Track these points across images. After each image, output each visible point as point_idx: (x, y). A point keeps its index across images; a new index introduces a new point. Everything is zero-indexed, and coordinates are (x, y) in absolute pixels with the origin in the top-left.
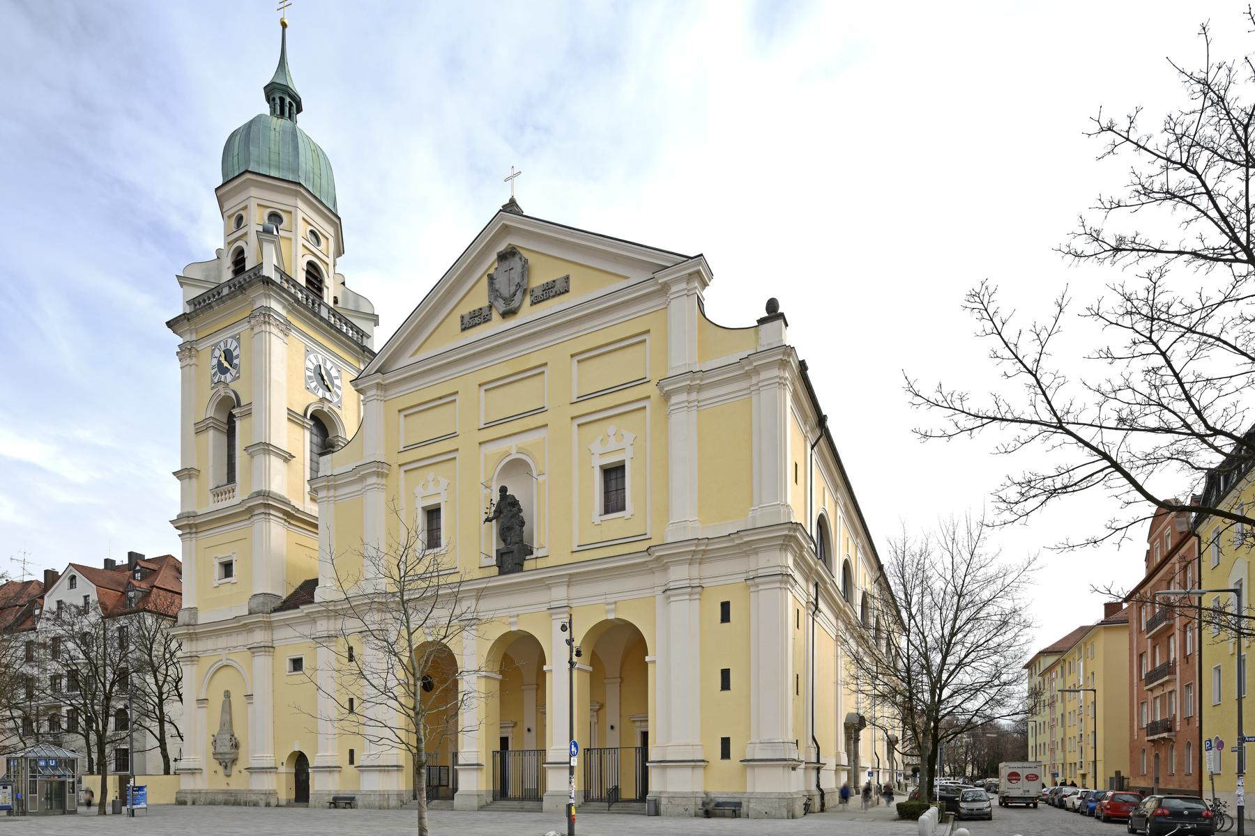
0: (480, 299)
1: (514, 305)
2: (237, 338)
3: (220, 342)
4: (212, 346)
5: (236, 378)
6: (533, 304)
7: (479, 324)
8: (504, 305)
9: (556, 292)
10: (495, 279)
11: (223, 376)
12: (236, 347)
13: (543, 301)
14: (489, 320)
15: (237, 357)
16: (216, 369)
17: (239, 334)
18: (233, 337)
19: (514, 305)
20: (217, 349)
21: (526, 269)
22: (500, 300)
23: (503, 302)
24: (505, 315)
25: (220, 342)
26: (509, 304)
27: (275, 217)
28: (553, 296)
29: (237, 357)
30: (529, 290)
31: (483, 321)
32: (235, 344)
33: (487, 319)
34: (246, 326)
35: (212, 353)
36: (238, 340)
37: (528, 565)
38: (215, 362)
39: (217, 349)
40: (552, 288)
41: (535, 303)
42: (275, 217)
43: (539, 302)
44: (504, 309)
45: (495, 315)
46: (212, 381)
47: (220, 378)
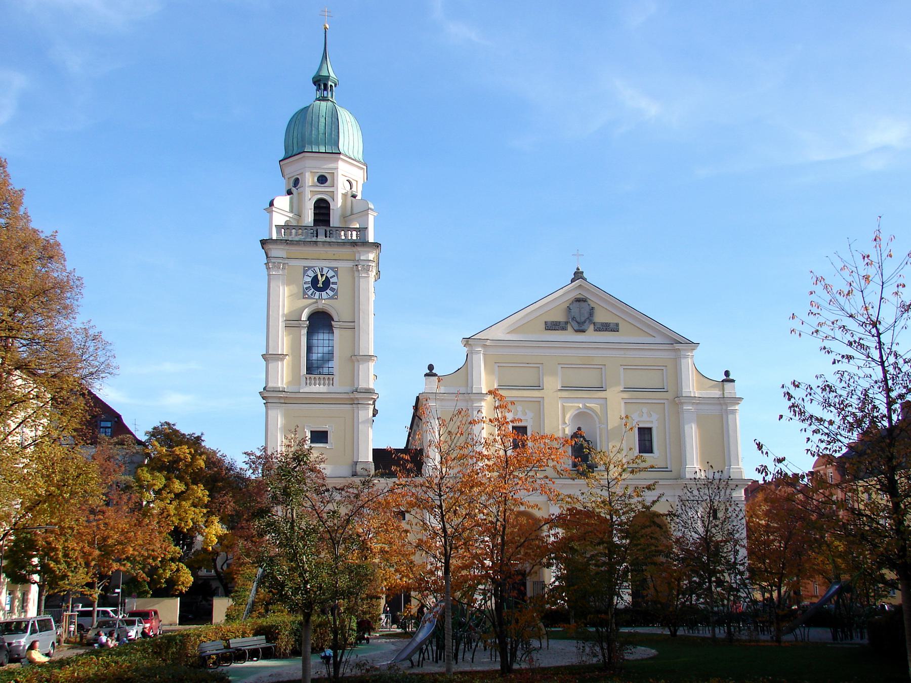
0: (560, 317)
1: (583, 327)
4: (304, 267)
5: (332, 298)
6: (595, 330)
12: (334, 276)
15: (333, 283)
17: (337, 268)
18: (332, 269)
19: (583, 327)
24: (577, 331)
34: (350, 264)
36: (336, 272)
38: (309, 279)
46: (305, 293)
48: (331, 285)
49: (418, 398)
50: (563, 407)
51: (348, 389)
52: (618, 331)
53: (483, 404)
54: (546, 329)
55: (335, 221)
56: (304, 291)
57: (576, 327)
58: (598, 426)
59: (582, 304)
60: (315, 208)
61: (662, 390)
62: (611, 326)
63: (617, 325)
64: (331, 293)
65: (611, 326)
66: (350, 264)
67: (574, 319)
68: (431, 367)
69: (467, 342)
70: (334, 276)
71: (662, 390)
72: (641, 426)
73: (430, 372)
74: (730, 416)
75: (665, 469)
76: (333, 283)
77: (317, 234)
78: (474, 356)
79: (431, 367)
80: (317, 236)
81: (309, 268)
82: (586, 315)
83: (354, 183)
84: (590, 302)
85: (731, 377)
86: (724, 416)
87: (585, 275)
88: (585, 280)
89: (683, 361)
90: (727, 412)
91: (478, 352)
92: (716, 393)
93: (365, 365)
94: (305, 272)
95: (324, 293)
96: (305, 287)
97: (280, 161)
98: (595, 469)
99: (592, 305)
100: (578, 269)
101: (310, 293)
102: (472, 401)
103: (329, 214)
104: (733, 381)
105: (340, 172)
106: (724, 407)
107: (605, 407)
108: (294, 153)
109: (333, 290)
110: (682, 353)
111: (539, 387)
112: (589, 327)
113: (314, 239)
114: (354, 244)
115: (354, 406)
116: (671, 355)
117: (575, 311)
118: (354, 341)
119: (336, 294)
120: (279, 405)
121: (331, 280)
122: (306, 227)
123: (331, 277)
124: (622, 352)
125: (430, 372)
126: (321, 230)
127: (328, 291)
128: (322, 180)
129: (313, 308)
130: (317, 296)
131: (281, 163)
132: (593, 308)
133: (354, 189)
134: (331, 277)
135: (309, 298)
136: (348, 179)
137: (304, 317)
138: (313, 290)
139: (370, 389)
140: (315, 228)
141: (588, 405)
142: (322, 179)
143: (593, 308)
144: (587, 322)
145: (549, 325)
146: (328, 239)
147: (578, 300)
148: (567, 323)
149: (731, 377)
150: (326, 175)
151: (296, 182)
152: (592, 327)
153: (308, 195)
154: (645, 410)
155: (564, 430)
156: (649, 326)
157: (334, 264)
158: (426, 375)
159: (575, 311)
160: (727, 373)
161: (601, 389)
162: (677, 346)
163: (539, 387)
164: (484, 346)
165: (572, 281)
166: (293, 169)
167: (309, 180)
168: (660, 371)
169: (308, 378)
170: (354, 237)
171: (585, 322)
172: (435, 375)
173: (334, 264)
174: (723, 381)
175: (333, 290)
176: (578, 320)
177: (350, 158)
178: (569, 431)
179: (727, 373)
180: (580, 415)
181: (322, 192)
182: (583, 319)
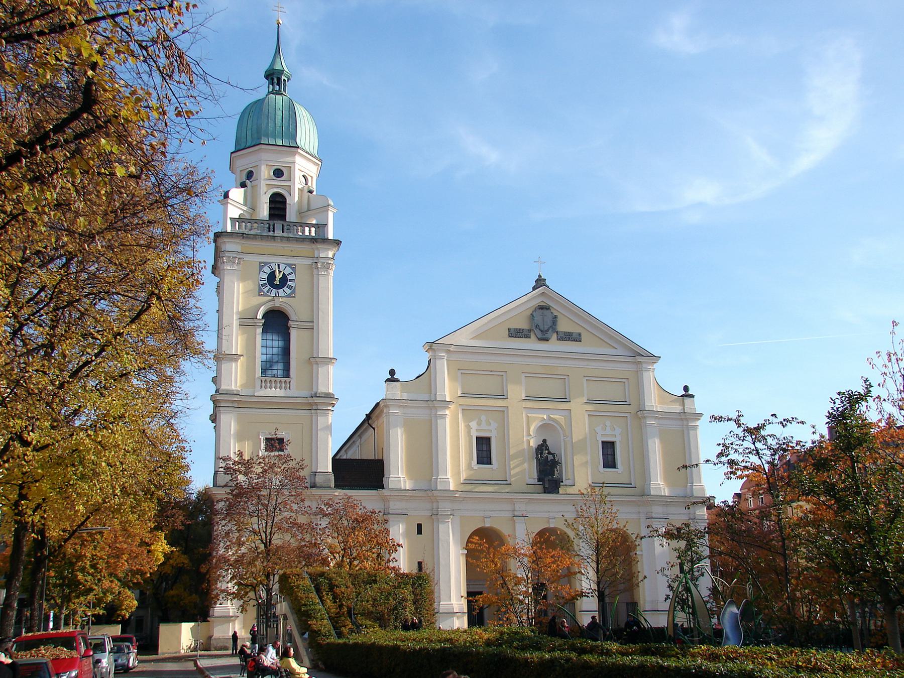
0: (523, 325)
1: (547, 336)
4: (260, 263)
5: (289, 296)
6: (558, 339)
12: (291, 273)
15: (291, 281)
16: (266, 282)
18: (290, 265)
19: (547, 336)
33: (528, 337)
34: (308, 262)
35: (261, 267)
36: (294, 269)
37: (561, 490)
38: (266, 276)
46: (260, 290)
48: (288, 283)
49: (378, 404)
51: (305, 393)
52: (580, 341)
53: (447, 412)
54: (509, 336)
55: (291, 216)
56: (259, 287)
57: (540, 335)
58: (562, 438)
59: (546, 312)
60: (271, 202)
61: (625, 403)
62: (574, 334)
63: (580, 335)
64: (288, 291)
66: (308, 262)
67: (537, 326)
68: (392, 372)
69: (431, 346)
70: (291, 273)
71: (625, 403)
72: (605, 440)
73: (392, 378)
74: (691, 432)
75: (628, 485)
76: (291, 281)
77: (274, 228)
78: (438, 362)
79: (392, 372)
80: (274, 231)
81: (266, 264)
82: (550, 324)
83: (309, 179)
84: (552, 310)
85: (690, 392)
86: (685, 432)
87: (547, 283)
88: (548, 287)
89: (645, 374)
90: (689, 428)
91: (441, 358)
92: (677, 408)
93: (325, 368)
94: (261, 267)
95: (280, 291)
97: (231, 153)
98: (561, 483)
99: (555, 313)
100: (540, 276)
101: (265, 290)
102: (436, 408)
103: (285, 209)
104: (692, 396)
105: (297, 167)
106: (685, 423)
107: (569, 419)
108: (248, 144)
109: (290, 287)
110: (644, 366)
111: (503, 396)
112: (552, 336)
113: (271, 233)
114: (313, 240)
115: (313, 411)
116: (632, 368)
117: (538, 319)
119: (294, 292)
120: (232, 409)
121: (289, 277)
122: (262, 222)
123: (289, 275)
124: (586, 363)
125: (392, 378)
126: (278, 224)
127: (285, 289)
128: (278, 174)
129: (269, 306)
130: (273, 294)
131: (233, 155)
132: (556, 317)
133: (310, 184)
134: (289, 275)
135: (265, 295)
136: (304, 174)
137: (260, 316)
138: (269, 287)
139: (330, 394)
140: (271, 223)
141: (552, 416)
142: (278, 173)
143: (556, 317)
145: (512, 332)
146: (285, 235)
147: (541, 308)
148: (530, 331)
149: (690, 392)
150: (282, 168)
151: (250, 175)
152: (555, 336)
153: (263, 188)
154: (608, 423)
155: (529, 442)
157: (291, 261)
158: (388, 380)
159: (538, 319)
160: (686, 388)
161: (565, 400)
162: (639, 359)
163: (503, 396)
164: (448, 351)
165: (534, 289)
166: (245, 161)
167: (265, 173)
168: (622, 384)
169: (263, 380)
170: (313, 234)
171: (548, 330)
172: (397, 380)
173: (291, 261)
174: (682, 396)
175: (290, 287)
176: (542, 329)
177: (307, 153)
178: (534, 443)
179: (686, 388)
180: (545, 427)
181: (278, 185)
182: (546, 327)
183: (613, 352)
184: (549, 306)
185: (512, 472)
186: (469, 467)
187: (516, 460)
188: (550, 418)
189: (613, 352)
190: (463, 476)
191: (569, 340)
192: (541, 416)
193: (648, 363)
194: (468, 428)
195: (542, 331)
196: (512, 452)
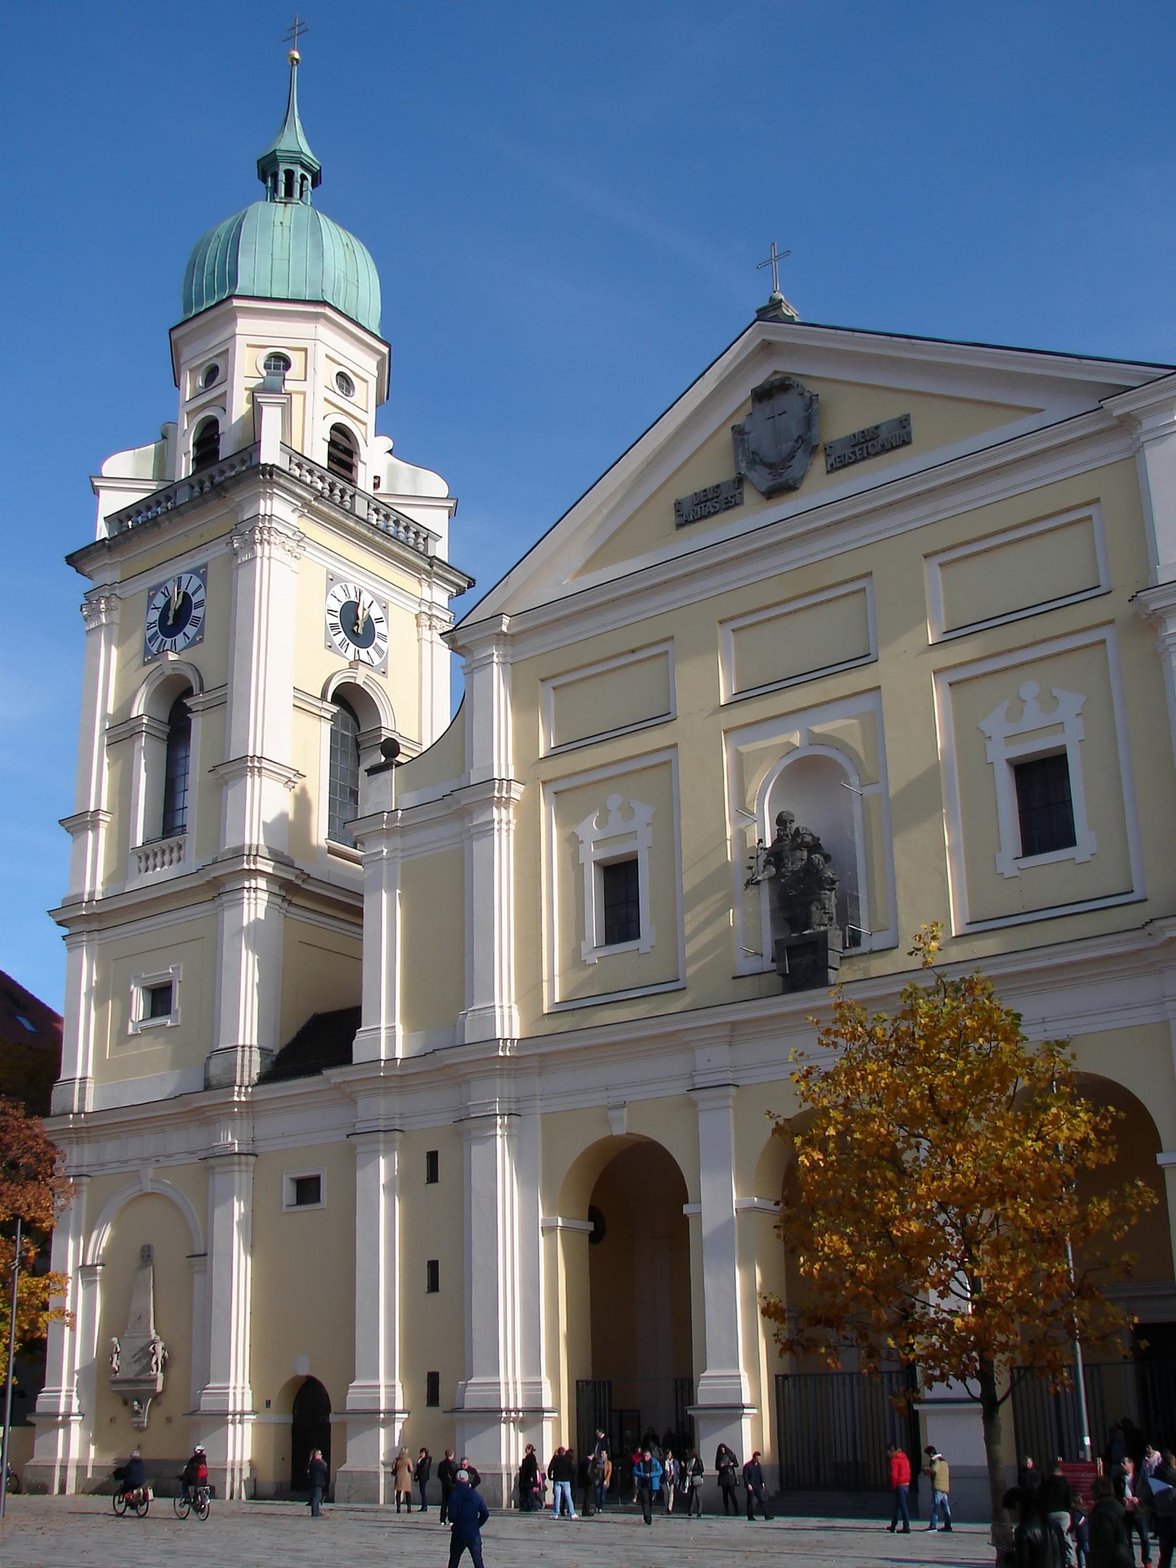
1: (789, 475)
2: (201, 573)
3: (169, 580)
4: (150, 590)
5: (193, 643)
6: (832, 469)
7: (715, 513)
8: (770, 477)
9: (883, 446)
10: (748, 433)
11: (169, 640)
13: (853, 463)
14: (736, 505)
15: (200, 604)
16: (157, 628)
17: (205, 566)
18: (195, 571)
20: (160, 594)
21: (811, 409)
22: (760, 468)
23: (768, 471)
24: (772, 494)
25: (169, 580)
26: (781, 475)
27: (279, 362)
28: (877, 454)
29: (200, 604)
30: (821, 447)
31: (724, 506)
32: (196, 581)
35: (151, 599)
36: (203, 577)
38: (155, 616)
39: (160, 594)
40: (872, 439)
41: (838, 468)
42: (279, 362)
43: (845, 466)
44: (771, 483)
45: (750, 496)
46: (147, 651)
47: (163, 643)
50: (739, 760)
61: (1093, 592)
62: (884, 434)
65: (884, 434)
67: (755, 460)
71: (1093, 592)
81: (156, 589)
94: (151, 599)
96: (148, 637)
99: (812, 387)
101: (154, 650)
107: (874, 725)
118: (223, 733)
121: (195, 600)
138: (162, 637)
141: (817, 729)
144: (799, 453)
147: (762, 395)
148: (740, 481)
152: (820, 463)
154: (1029, 688)
156: (1012, 379)
161: (865, 659)
171: (792, 456)
176: (771, 455)
182: (786, 447)
183: (1032, 422)
184: (788, 376)
185: (690, 949)
186: (574, 960)
187: (699, 908)
188: (813, 739)
189: (1032, 422)
190: (554, 991)
191: (869, 456)
192: (780, 739)
193: (1154, 409)
194: (572, 842)
195: (770, 466)
196: (688, 882)
